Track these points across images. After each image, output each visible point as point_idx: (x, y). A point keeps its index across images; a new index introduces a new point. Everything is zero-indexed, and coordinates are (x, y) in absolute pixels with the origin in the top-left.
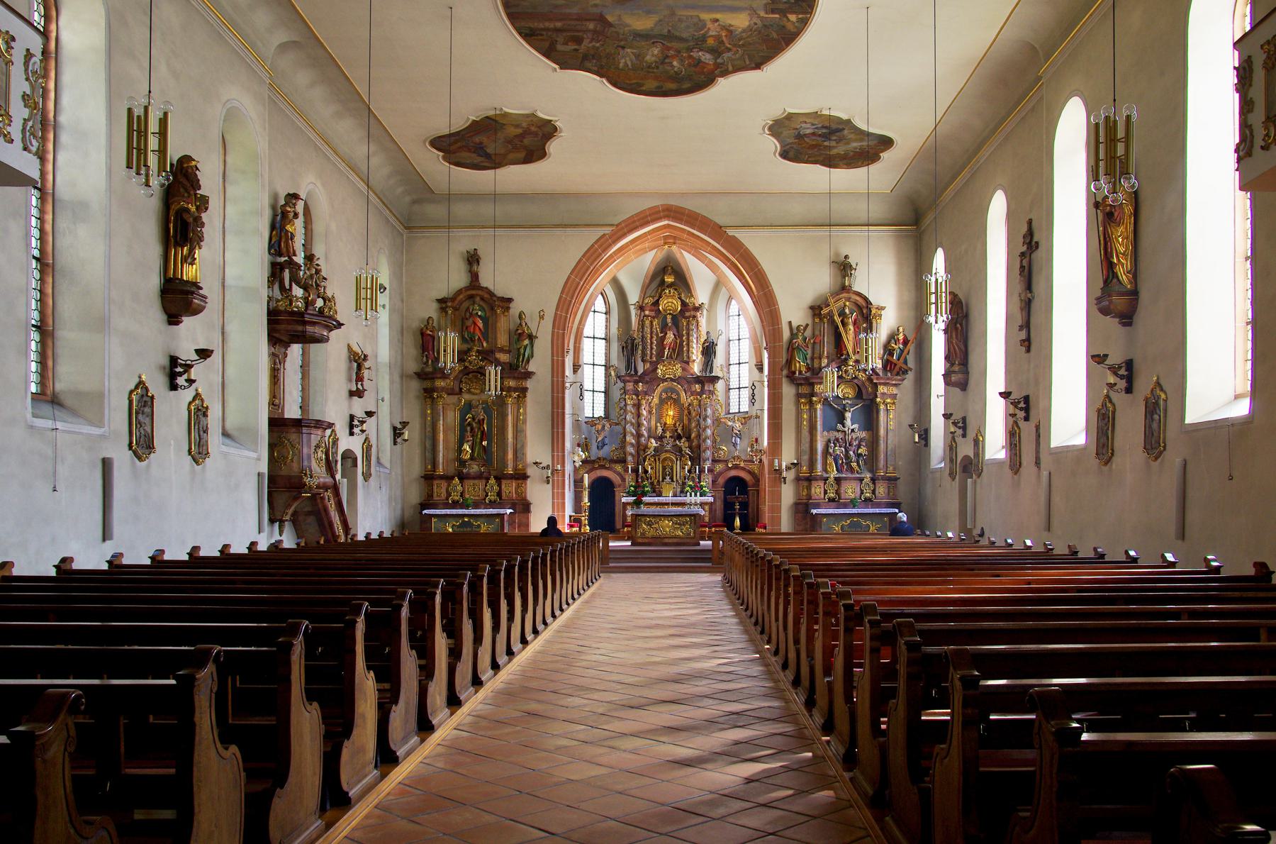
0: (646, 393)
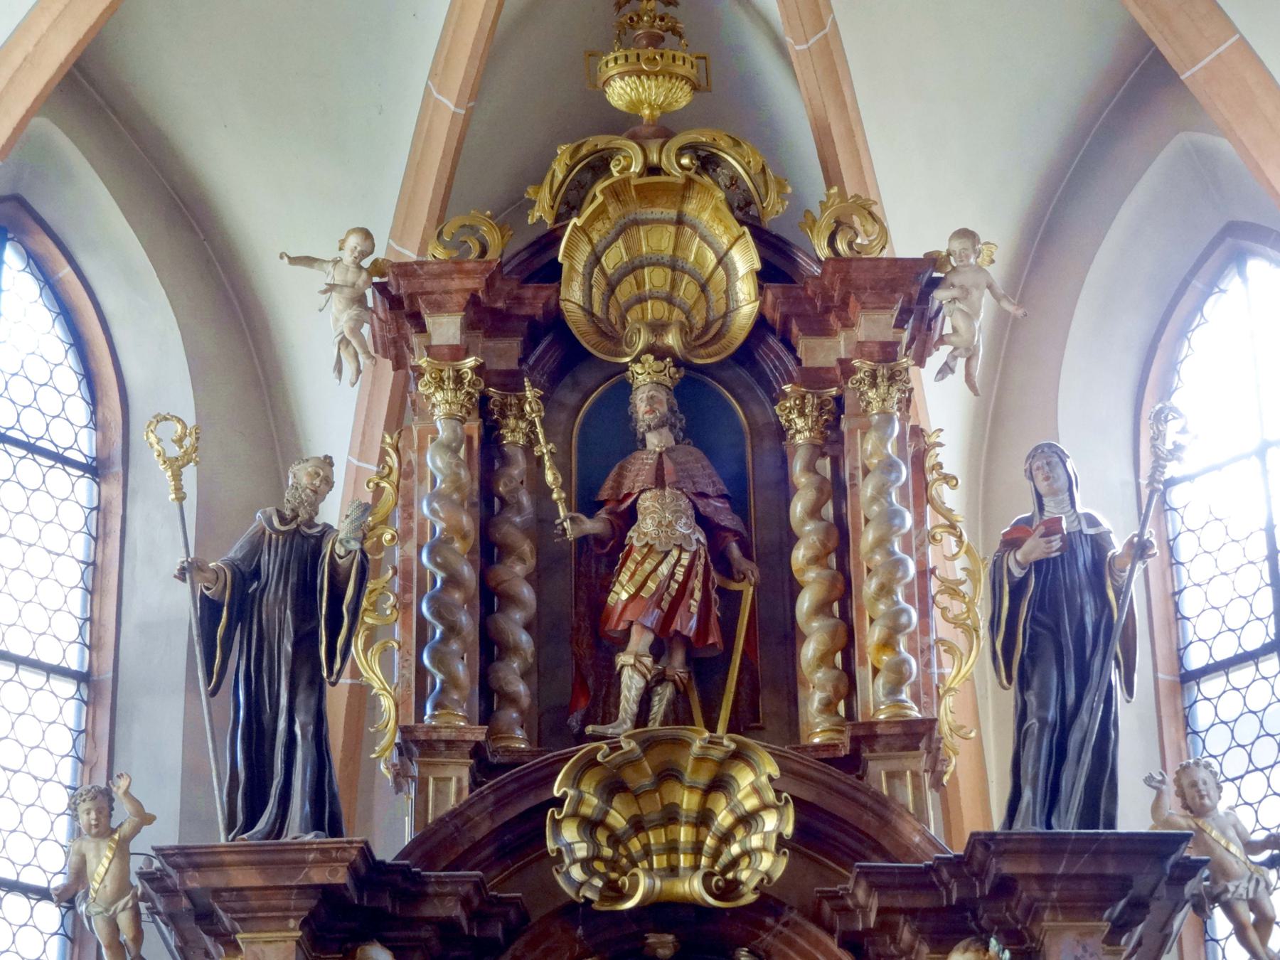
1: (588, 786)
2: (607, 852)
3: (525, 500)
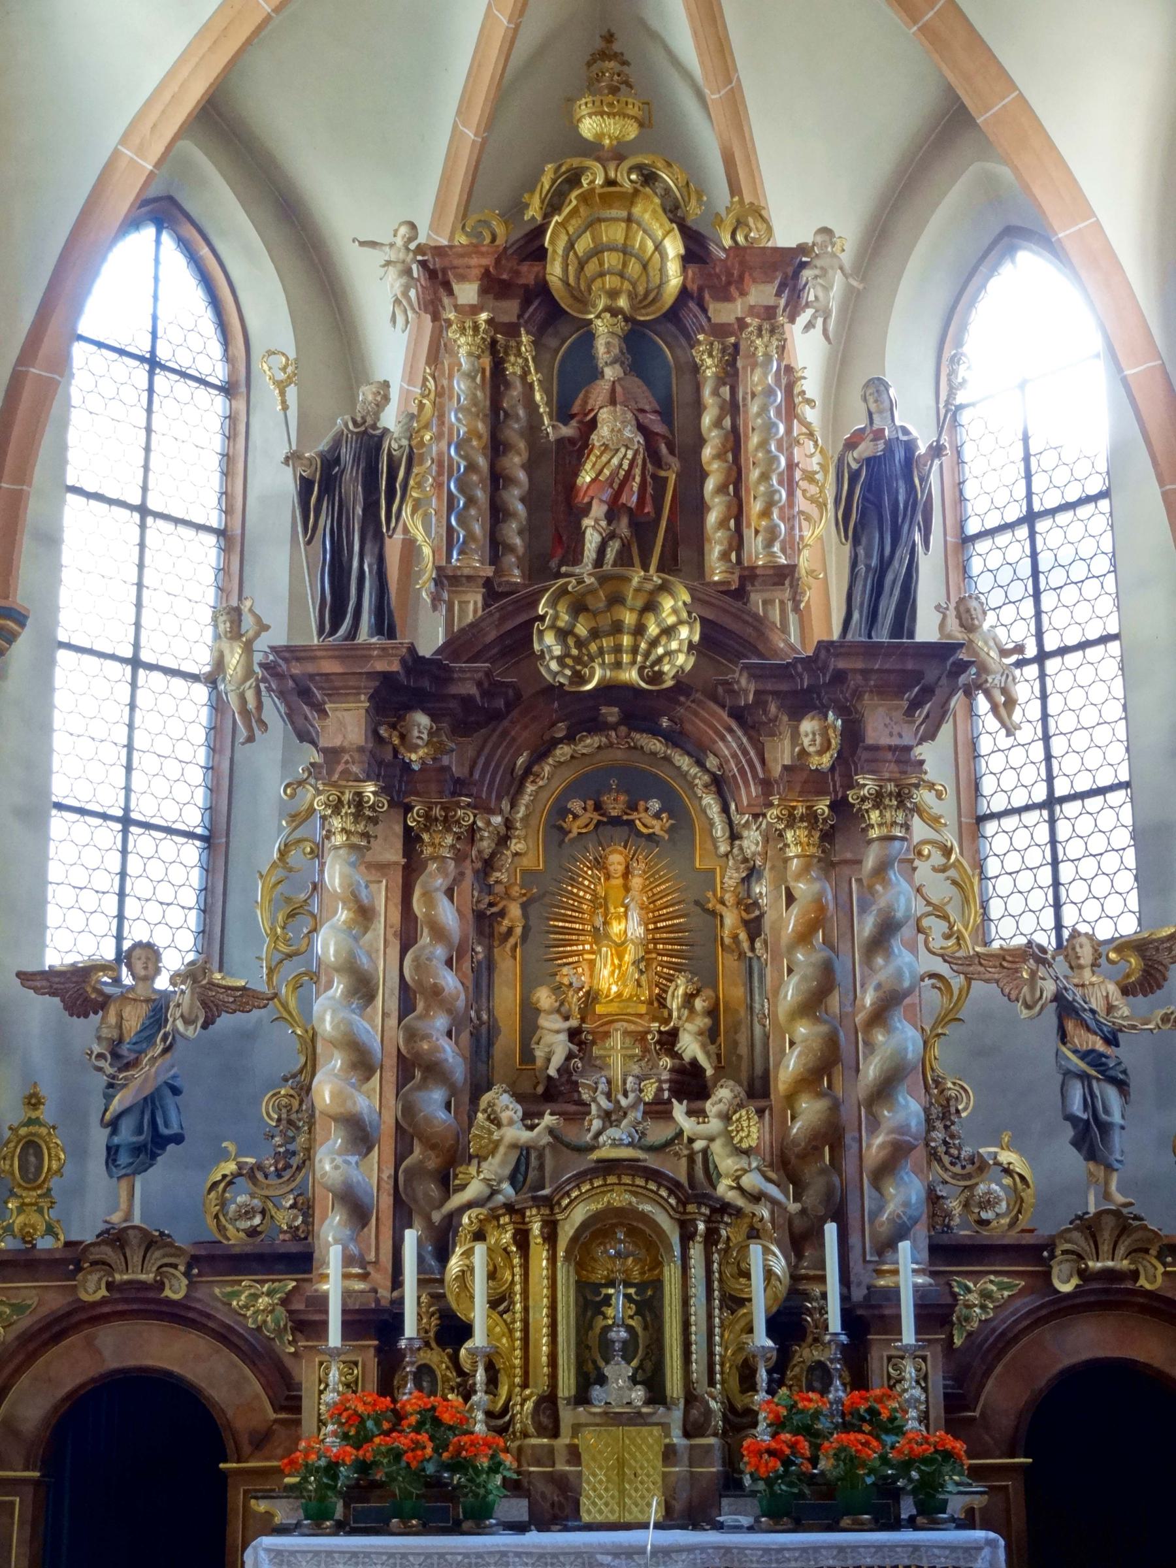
0: (460, 786)
1: (562, 608)
2: (575, 652)
3: (521, 413)
